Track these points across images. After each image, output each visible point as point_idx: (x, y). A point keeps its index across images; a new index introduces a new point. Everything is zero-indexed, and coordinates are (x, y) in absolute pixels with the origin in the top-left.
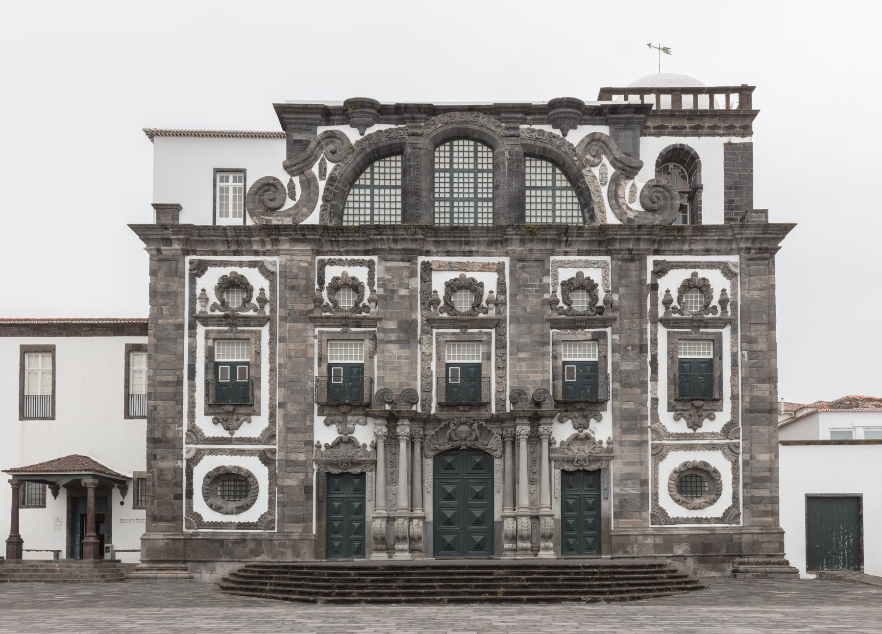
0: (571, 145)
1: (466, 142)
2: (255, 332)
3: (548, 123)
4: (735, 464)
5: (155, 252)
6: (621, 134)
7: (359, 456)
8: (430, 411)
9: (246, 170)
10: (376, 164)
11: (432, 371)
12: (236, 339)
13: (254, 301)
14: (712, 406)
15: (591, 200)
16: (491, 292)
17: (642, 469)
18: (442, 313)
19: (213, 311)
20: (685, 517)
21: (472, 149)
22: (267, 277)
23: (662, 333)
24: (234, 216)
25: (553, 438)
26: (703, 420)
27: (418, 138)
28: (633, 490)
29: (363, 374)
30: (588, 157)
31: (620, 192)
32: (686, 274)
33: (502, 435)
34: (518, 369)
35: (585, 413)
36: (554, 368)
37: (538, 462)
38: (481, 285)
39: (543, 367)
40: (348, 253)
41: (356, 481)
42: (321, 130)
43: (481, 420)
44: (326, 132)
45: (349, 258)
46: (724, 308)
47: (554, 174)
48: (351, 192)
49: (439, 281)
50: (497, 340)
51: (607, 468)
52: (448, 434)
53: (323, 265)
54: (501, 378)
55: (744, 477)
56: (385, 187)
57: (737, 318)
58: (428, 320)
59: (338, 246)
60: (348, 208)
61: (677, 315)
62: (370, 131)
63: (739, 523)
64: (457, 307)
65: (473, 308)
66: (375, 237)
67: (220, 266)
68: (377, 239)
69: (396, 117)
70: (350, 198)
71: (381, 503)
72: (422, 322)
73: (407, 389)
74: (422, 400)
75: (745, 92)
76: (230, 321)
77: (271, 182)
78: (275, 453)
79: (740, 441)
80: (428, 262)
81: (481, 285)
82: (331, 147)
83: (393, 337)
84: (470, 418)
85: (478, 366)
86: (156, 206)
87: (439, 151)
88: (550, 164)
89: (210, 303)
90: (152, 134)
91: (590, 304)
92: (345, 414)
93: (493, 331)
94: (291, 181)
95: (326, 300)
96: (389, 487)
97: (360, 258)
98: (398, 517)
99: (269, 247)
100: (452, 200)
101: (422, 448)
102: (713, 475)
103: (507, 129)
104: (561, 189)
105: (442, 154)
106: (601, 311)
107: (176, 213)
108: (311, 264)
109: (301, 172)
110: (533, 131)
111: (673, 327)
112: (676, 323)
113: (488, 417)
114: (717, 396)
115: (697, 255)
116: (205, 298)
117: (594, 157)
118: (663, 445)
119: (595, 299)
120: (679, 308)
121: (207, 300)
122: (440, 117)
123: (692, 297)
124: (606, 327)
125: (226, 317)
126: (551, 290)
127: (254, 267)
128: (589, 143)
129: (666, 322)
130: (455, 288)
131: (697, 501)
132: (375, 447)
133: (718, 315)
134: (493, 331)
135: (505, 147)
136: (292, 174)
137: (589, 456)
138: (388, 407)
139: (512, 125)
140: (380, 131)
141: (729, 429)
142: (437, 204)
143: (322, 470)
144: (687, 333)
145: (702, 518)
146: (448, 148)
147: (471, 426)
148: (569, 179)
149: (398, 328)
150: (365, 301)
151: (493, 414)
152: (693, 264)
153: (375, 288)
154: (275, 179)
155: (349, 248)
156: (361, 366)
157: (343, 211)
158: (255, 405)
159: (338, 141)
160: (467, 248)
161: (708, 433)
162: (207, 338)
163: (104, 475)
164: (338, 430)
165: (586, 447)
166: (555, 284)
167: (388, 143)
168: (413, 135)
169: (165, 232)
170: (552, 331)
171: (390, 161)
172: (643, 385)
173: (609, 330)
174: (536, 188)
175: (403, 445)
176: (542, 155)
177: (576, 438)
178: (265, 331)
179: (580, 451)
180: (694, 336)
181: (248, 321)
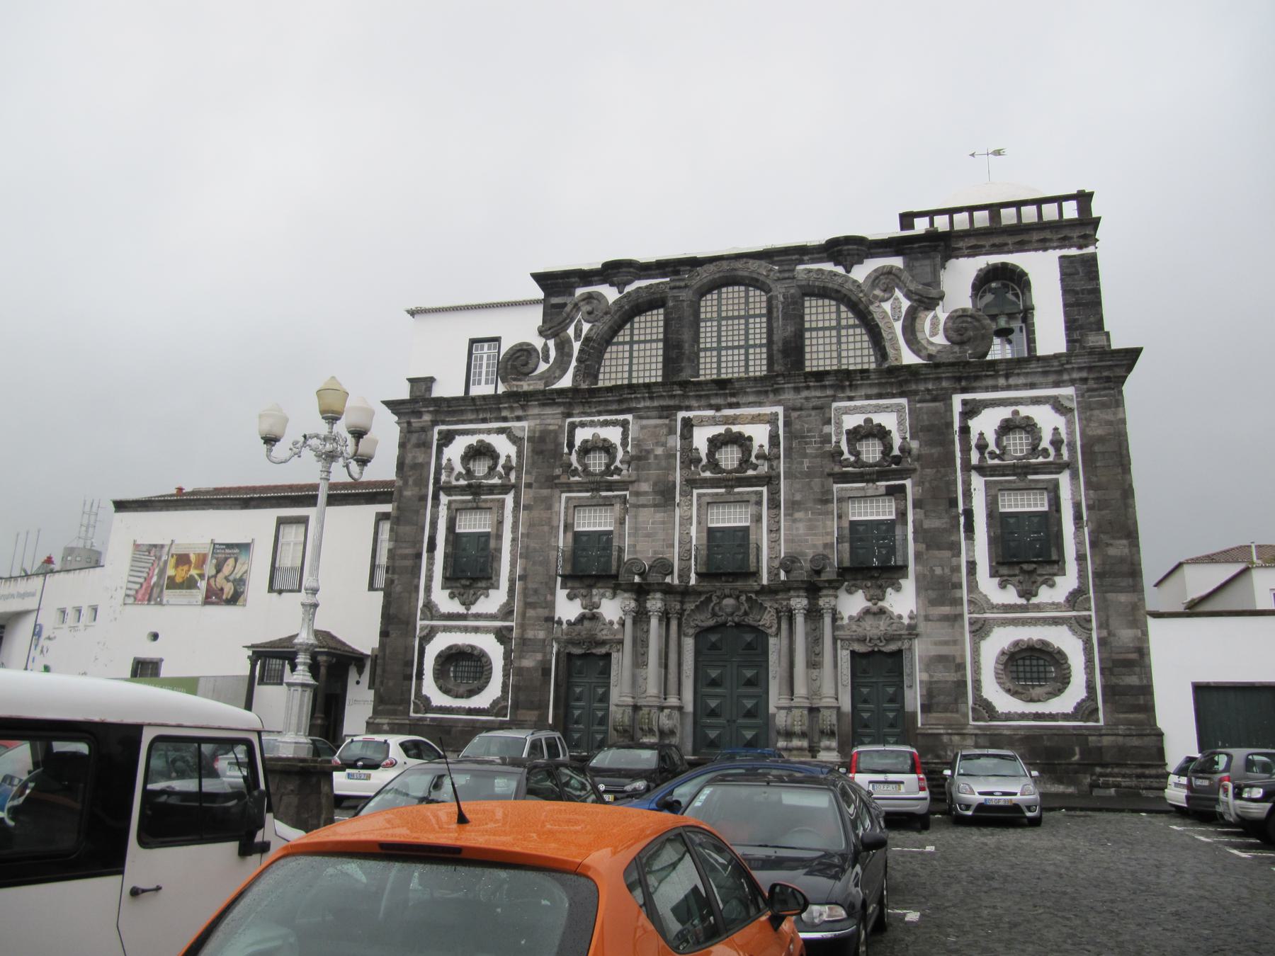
0: (855, 281)
2: (498, 500)
3: (829, 259)
5: (405, 425)
6: (917, 264)
7: (604, 635)
8: (689, 582)
10: (637, 319)
11: (691, 537)
12: (478, 508)
13: (499, 468)
14: (1048, 569)
15: (883, 338)
16: (761, 446)
18: (704, 471)
19: (457, 480)
20: (1019, 712)
21: (742, 294)
24: (487, 383)
25: (840, 613)
26: (1038, 588)
28: (945, 676)
29: (612, 543)
30: (877, 292)
31: (918, 326)
33: (776, 609)
34: (794, 532)
35: (879, 583)
37: (820, 640)
38: (750, 439)
39: (825, 527)
40: (600, 413)
41: (601, 663)
45: (602, 418)
46: (1058, 450)
47: (838, 312)
48: (609, 350)
49: (701, 438)
50: (768, 499)
51: (910, 649)
52: (710, 608)
53: (573, 427)
54: (774, 542)
55: (1101, 660)
56: (645, 342)
57: (1077, 461)
58: (686, 481)
59: (590, 407)
60: (605, 366)
61: (996, 461)
62: (629, 289)
63: (1097, 720)
64: (723, 464)
65: (740, 464)
68: (631, 398)
69: (657, 272)
70: (607, 356)
71: (626, 688)
72: (681, 482)
73: (661, 558)
74: (680, 570)
75: (1084, 199)
76: (473, 490)
77: (525, 347)
78: (512, 630)
79: (1093, 613)
80: (689, 418)
81: (750, 439)
82: (588, 308)
84: (736, 589)
85: (745, 530)
86: (410, 380)
87: (706, 300)
88: (833, 303)
89: (456, 472)
90: (413, 313)
91: (882, 453)
92: (591, 587)
93: (765, 489)
94: (546, 345)
95: (575, 464)
96: (638, 671)
97: (614, 417)
98: (645, 706)
99: (519, 413)
100: (719, 349)
101: (679, 625)
104: (848, 327)
105: (709, 303)
106: (897, 460)
107: (429, 385)
108: (561, 427)
109: (555, 335)
110: (810, 271)
111: (992, 476)
112: (994, 471)
113: (757, 588)
114: (1054, 557)
115: (1017, 390)
116: (451, 469)
117: (885, 291)
118: (985, 620)
119: (888, 448)
120: (998, 452)
121: (452, 469)
122: (706, 267)
123: (1015, 439)
124: (905, 479)
125: (469, 486)
126: (834, 439)
127: (502, 433)
128: (877, 278)
129: (981, 470)
130: (718, 444)
131: (1037, 691)
132: (623, 624)
133: (1051, 459)
134: (765, 489)
135: (779, 290)
136: (547, 337)
137: (885, 634)
138: (637, 579)
139: (786, 268)
140: (640, 288)
141: (1075, 598)
142: (702, 354)
143: (562, 650)
144: (1013, 482)
145: (1044, 714)
146: (715, 296)
147: (738, 598)
150: (618, 463)
151: (763, 585)
152: (1012, 400)
153: (629, 449)
154: (529, 344)
155: (601, 408)
156: (610, 532)
157: (599, 369)
158: (494, 578)
159: (595, 301)
160: (734, 400)
161: (1047, 604)
162: (449, 508)
163: (339, 652)
164: (582, 605)
165: (882, 623)
166: (838, 434)
167: (649, 298)
170: (836, 486)
172: (955, 548)
173: (908, 483)
174: (817, 329)
175: (654, 622)
176: (823, 292)
177: (867, 612)
178: (509, 499)
179: (873, 628)
180: (1022, 485)
181: (492, 489)
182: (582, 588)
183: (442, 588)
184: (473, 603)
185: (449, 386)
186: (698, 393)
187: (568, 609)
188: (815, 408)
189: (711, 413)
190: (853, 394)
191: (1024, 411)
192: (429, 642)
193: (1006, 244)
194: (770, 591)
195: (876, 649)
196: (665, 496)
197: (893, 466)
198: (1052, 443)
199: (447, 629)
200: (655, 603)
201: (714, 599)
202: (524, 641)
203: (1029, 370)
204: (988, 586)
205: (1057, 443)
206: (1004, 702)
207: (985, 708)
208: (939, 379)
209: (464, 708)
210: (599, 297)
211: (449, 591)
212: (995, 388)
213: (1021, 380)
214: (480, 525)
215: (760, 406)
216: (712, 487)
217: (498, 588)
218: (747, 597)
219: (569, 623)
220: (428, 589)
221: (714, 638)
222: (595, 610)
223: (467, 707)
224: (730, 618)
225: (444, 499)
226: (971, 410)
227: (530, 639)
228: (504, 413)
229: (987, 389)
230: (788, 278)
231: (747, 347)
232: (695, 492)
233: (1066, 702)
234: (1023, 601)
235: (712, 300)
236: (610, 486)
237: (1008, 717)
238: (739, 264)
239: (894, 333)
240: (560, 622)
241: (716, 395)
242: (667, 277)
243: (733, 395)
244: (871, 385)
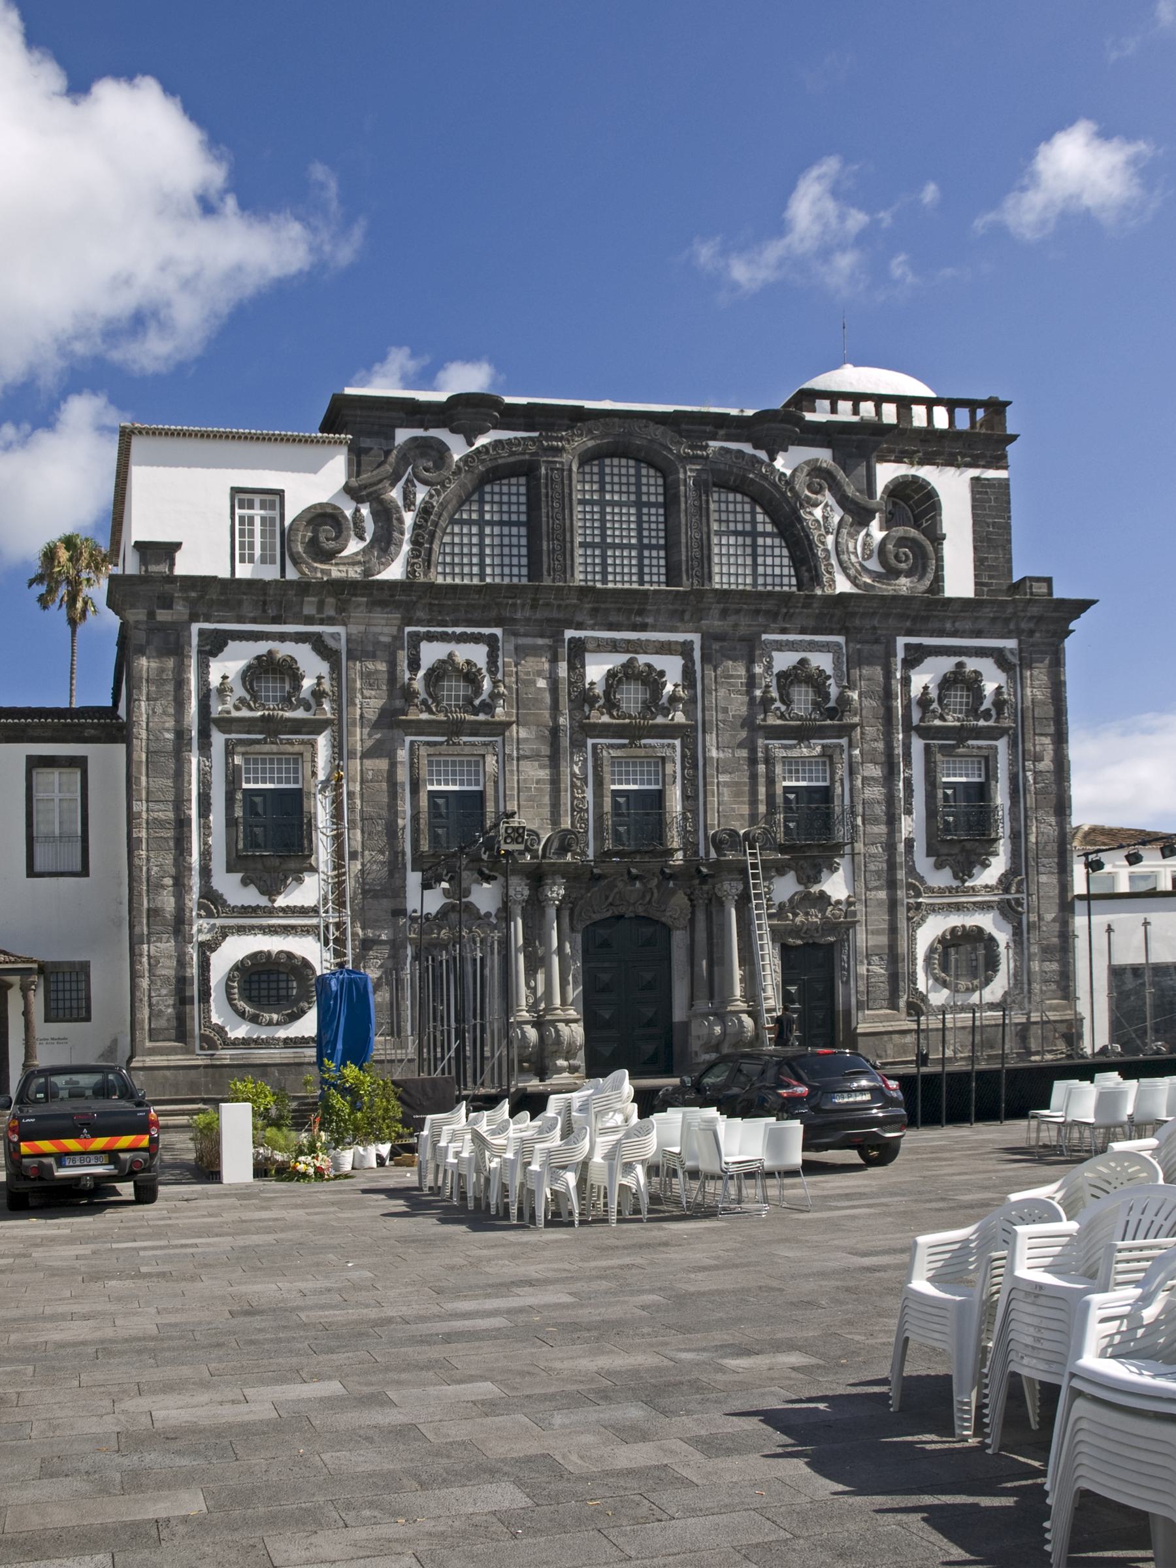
1: (624, 461)
9: (283, 491)
21: (632, 471)
32: (946, 664)
38: (662, 674)
42: (402, 435)
45: (458, 630)
46: (1000, 712)
49: (596, 671)
53: (416, 639)
62: (482, 441)
66: (505, 601)
67: (247, 639)
77: (329, 510)
88: (747, 499)
93: (677, 742)
94: (357, 510)
97: (476, 630)
104: (765, 535)
106: (832, 713)
119: (826, 696)
127: (304, 642)
129: (925, 732)
134: (677, 742)
146: (596, 469)
148: (774, 522)
149: (537, 738)
159: (433, 453)
160: (639, 619)
169: (167, 587)
171: (509, 485)
176: (740, 486)
178: (323, 742)
181: (297, 726)
183: (230, 869)
191: (972, 664)
192: (213, 950)
199: (241, 930)
200: (556, 892)
208: (887, 616)
211: (240, 875)
212: (941, 633)
213: (968, 625)
215: (671, 631)
216: (613, 737)
220: (206, 872)
222: (464, 900)
225: (218, 739)
226: (915, 657)
229: (932, 634)
231: (641, 547)
232: (590, 742)
235: (592, 473)
241: (619, 610)
243: (641, 612)
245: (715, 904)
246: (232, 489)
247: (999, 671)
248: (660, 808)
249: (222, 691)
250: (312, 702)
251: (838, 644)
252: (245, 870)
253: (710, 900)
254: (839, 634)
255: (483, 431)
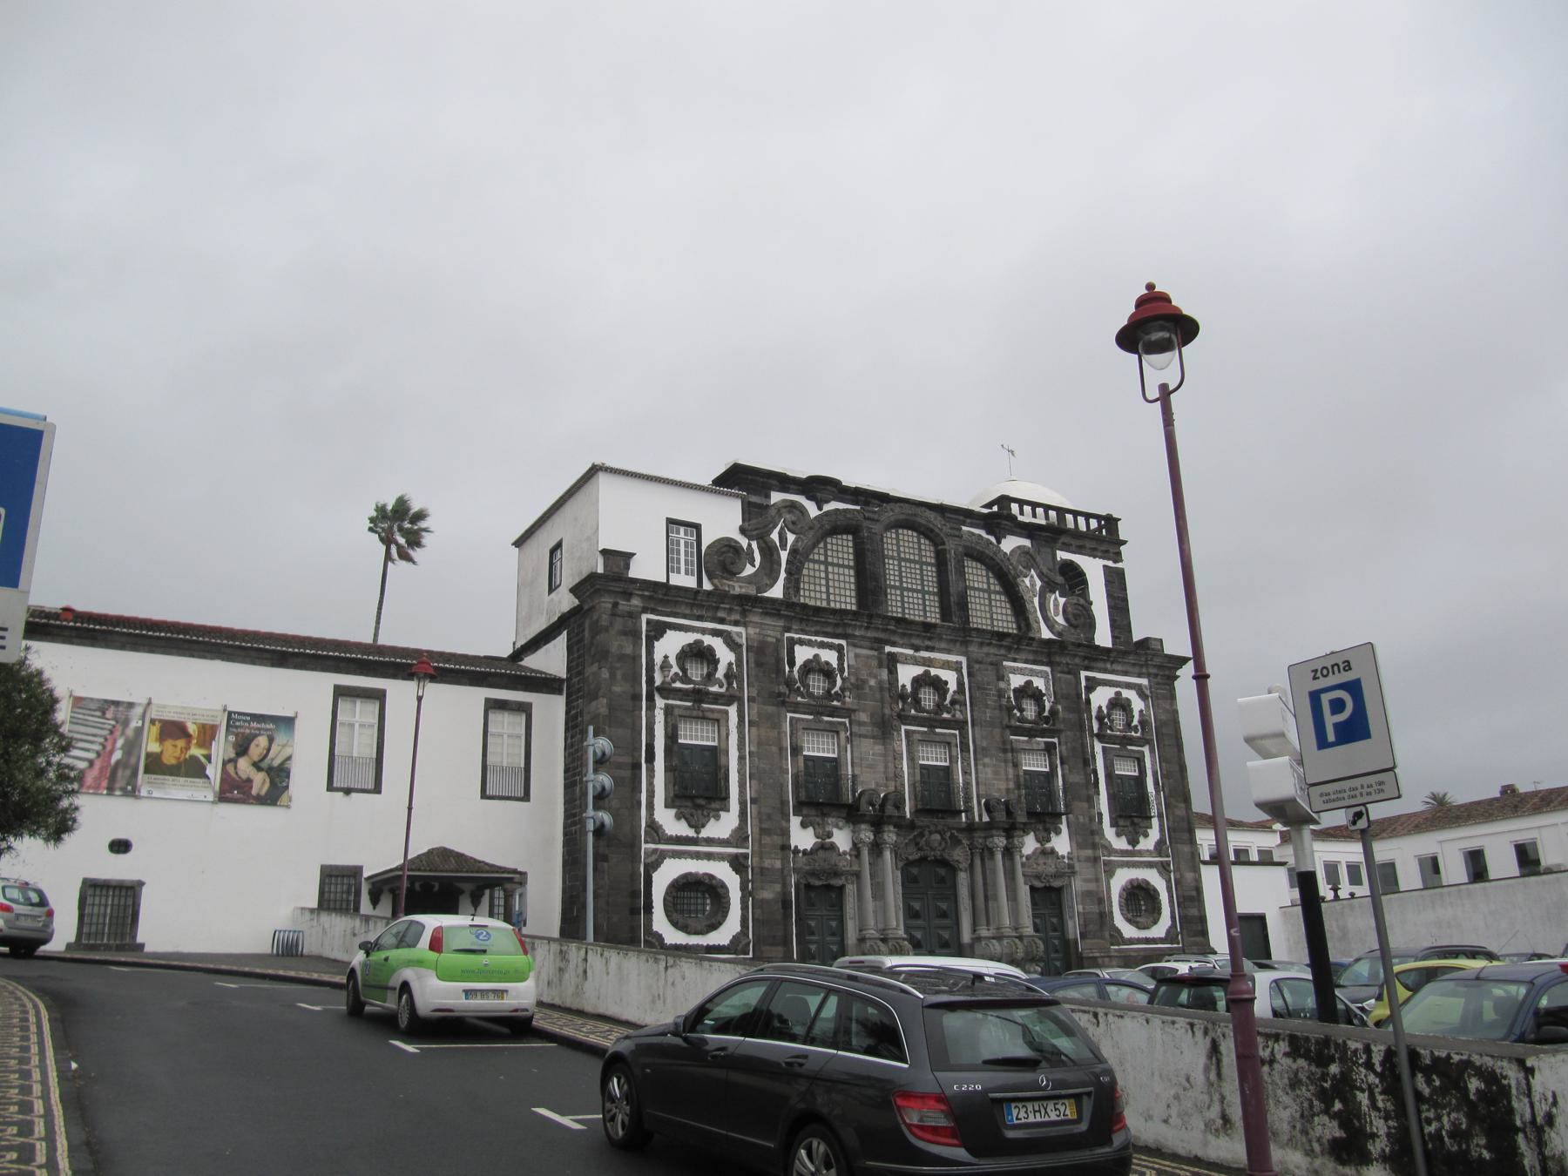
0: (1006, 553)
1: (910, 532)
4: (1168, 882)
12: (704, 718)
13: (720, 674)
17: (1098, 886)
22: (732, 649)
23: (1098, 747)
27: (874, 523)
36: (1017, 776)
38: (946, 682)
40: (817, 634)
43: (954, 829)
44: (784, 501)
45: (819, 639)
47: (987, 575)
49: (907, 674)
53: (792, 643)
62: (827, 507)
81: (946, 682)
83: (863, 730)
92: (824, 815)
94: (750, 545)
97: (830, 640)
102: (1152, 893)
103: (951, 528)
110: (973, 534)
116: (665, 665)
119: (1041, 707)
129: (1101, 737)
133: (1139, 735)
134: (957, 732)
136: (750, 538)
140: (837, 510)
146: (894, 536)
150: (837, 689)
153: (846, 674)
155: (818, 628)
168: (869, 519)
175: (888, 855)
178: (733, 711)
181: (717, 698)
182: (817, 816)
184: (703, 826)
185: (648, 567)
186: (906, 631)
187: (802, 838)
188: (991, 664)
189: (910, 652)
190: (1017, 657)
191: (1126, 693)
192: (655, 870)
193: (1071, 545)
194: (971, 828)
195: (1047, 885)
196: (884, 730)
197: (1045, 725)
198: (1139, 722)
200: (890, 836)
201: (926, 833)
202: (762, 872)
203: (1127, 661)
204: (1109, 832)
205: (1144, 723)
206: (1128, 931)
207: (1117, 936)
209: (702, 945)
210: (803, 511)
212: (1105, 671)
214: (702, 737)
215: (949, 654)
216: (918, 726)
217: (729, 811)
218: (952, 834)
219: (805, 852)
221: (915, 871)
222: (828, 840)
223: (705, 944)
224: (932, 853)
225: (660, 702)
226: (1092, 685)
227: (768, 869)
228: (721, 614)
230: (956, 536)
233: (1159, 930)
234: (1130, 848)
236: (834, 712)
237: (1131, 941)
238: (919, 510)
239: (1034, 607)
240: (796, 851)
241: (918, 636)
242: (857, 504)
244: (1030, 651)
245: (988, 852)
246: (667, 518)
247: (1140, 700)
248: (949, 780)
249: (665, 665)
250: (724, 681)
251: (1046, 672)
252: (678, 807)
253: (983, 849)
254: (1047, 665)
255: (827, 502)
